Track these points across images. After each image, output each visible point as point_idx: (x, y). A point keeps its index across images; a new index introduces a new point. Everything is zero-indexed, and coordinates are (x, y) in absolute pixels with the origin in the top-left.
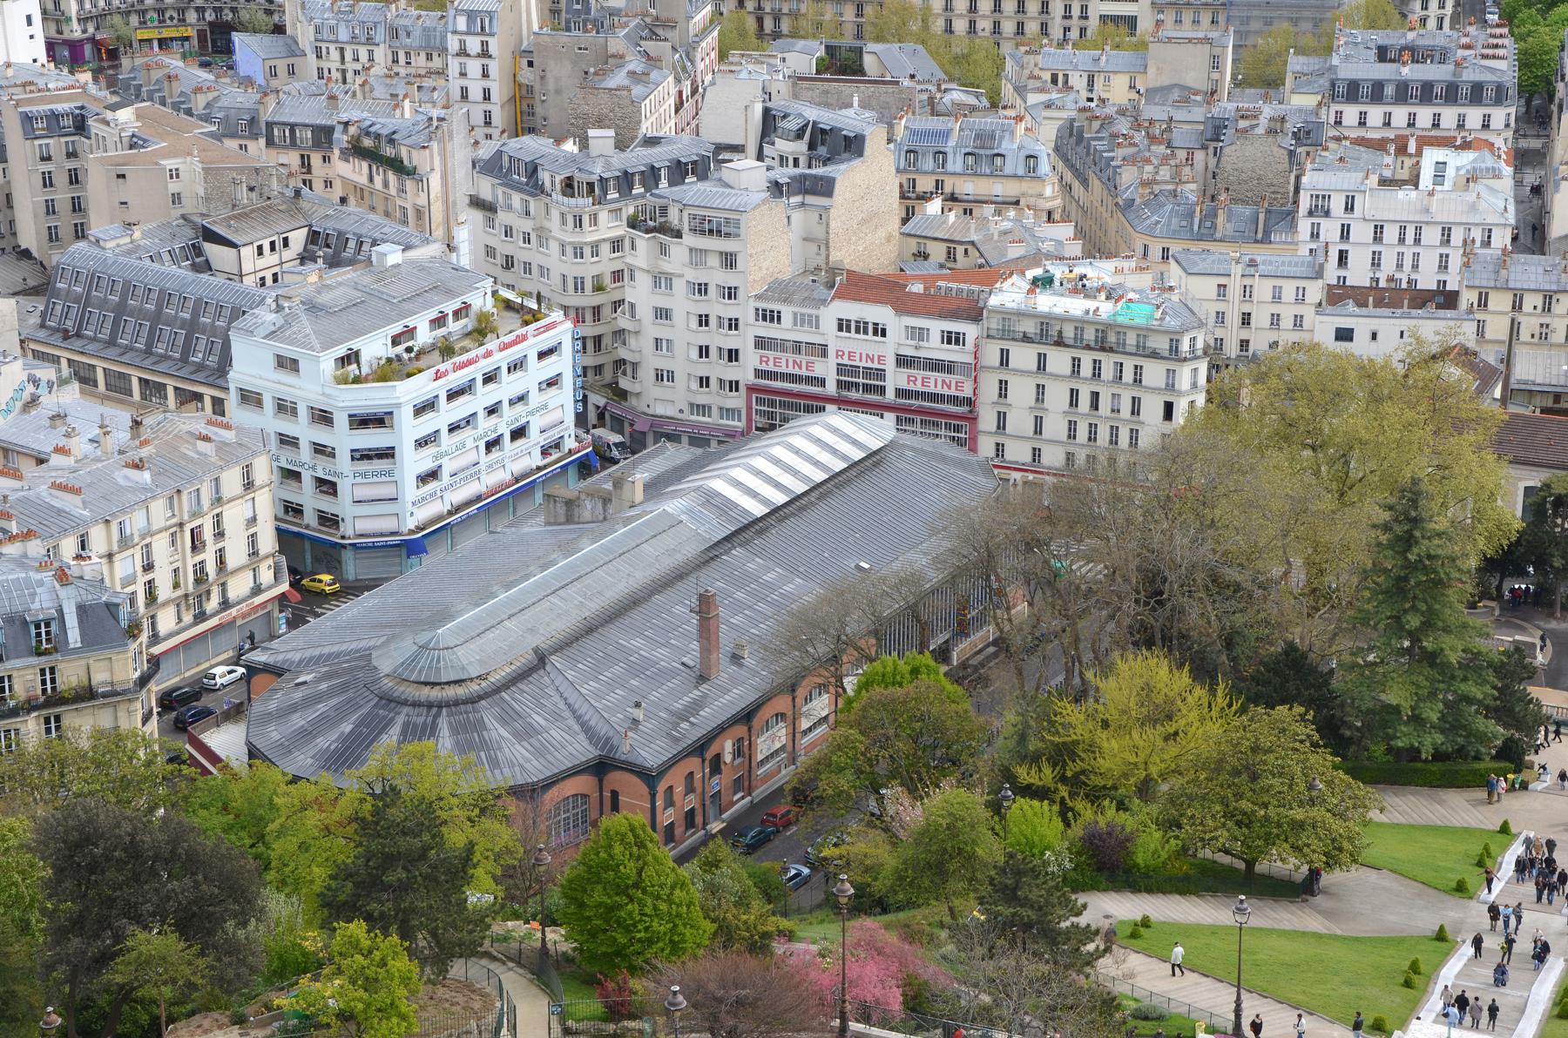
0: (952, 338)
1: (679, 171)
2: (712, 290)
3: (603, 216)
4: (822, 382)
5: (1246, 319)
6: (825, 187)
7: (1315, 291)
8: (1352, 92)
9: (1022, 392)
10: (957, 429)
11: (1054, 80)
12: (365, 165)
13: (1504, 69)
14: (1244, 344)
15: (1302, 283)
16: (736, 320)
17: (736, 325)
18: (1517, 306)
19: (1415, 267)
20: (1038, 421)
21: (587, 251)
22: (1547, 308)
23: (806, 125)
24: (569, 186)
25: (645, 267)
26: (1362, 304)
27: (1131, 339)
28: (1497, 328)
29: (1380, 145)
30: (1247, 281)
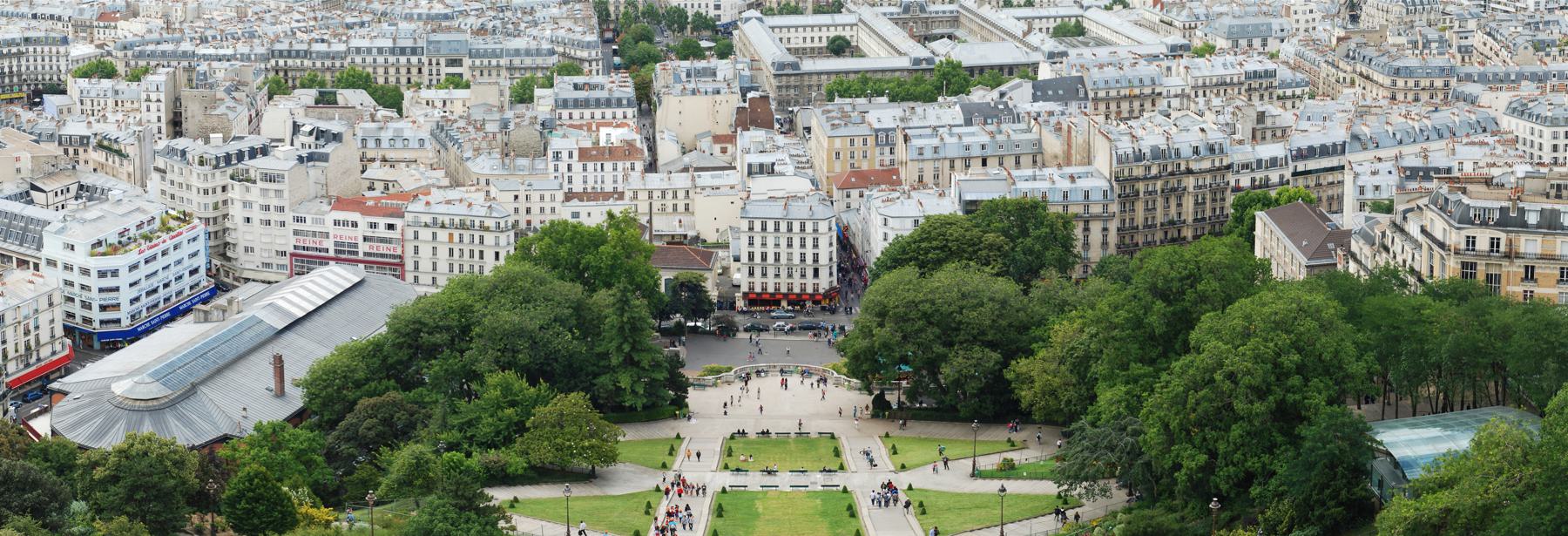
0: (391, 227)
1: (253, 153)
2: (272, 208)
4: (327, 251)
5: (528, 211)
7: (560, 196)
8: (565, 104)
9: (425, 251)
10: (395, 270)
11: (428, 104)
13: (629, 91)
14: (529, 223)
15: (553, 192)
18: (650, 197)
19: (603, 182)
20: (434, 264)
22: (664, 196)
24: (201, 163)
26: (581, 200)
27: (477, 223)
28: (643, 207)
29: (580, 127)
30: (528, 193)
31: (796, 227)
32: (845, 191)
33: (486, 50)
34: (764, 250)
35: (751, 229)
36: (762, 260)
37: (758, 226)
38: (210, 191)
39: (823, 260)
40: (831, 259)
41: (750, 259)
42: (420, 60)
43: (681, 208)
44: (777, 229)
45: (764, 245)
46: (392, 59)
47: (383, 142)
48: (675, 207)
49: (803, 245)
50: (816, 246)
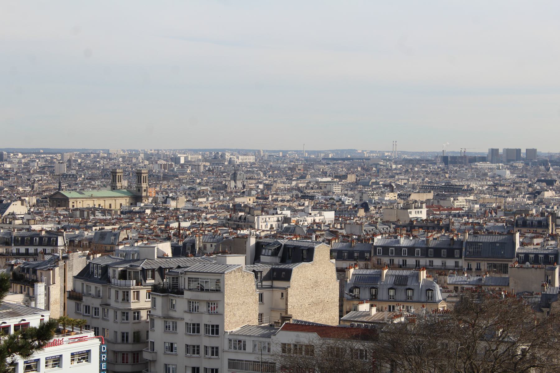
6: (286, 276)
11: (456, 289)
12: (19, 286)
16: (217, 348)
17: (217, 352)
23: (279, 249)
33: (536, 255)
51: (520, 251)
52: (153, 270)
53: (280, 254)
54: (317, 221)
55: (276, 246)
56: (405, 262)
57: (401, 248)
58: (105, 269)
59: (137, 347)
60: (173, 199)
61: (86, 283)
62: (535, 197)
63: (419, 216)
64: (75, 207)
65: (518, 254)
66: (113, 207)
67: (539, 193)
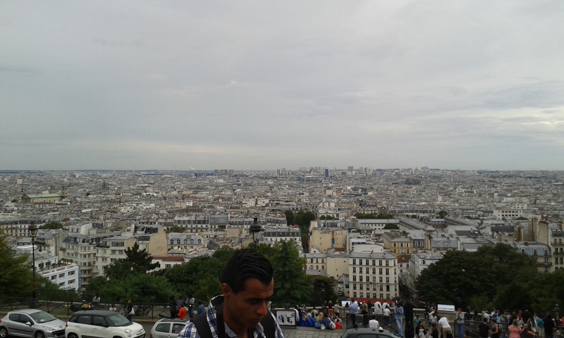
3: (92, 247)
11: (207, 237)
21: (87, 256)
22: (312, 262)
24: (84, 241)
25: (100, 256)
31: (377, 263)
32: (400, 263)
33: (236, 222)
34: (361, 275)
35: (354, 263)
36: (360, 280)
37: (358, 262)
38: (87, 256)
39: (392, 281)
40: (395, 281)
41: (354, 280)
42: (207, 226)
43: (320, 268)
44: (367, 264)
45: (361, 272)
46: (194, 226)
47: (181, 241)
48: (317, 267)
49: (381, 273)
50: (387, 273)
51: (230, 220)
52: (96, 239)
53: (145, 230)
54: (148, 208)
55: (143, 227)
56: (187, 226)
57: (185, 221)
58: (75, 239)
59: (90, 268)
60: (79, 197)
61: (68, 244)
62: (234, 191)
63: (189, 205)
64: (34, 202)
65: (229, 222)
66: (51, 201)
67: (235, 190)
